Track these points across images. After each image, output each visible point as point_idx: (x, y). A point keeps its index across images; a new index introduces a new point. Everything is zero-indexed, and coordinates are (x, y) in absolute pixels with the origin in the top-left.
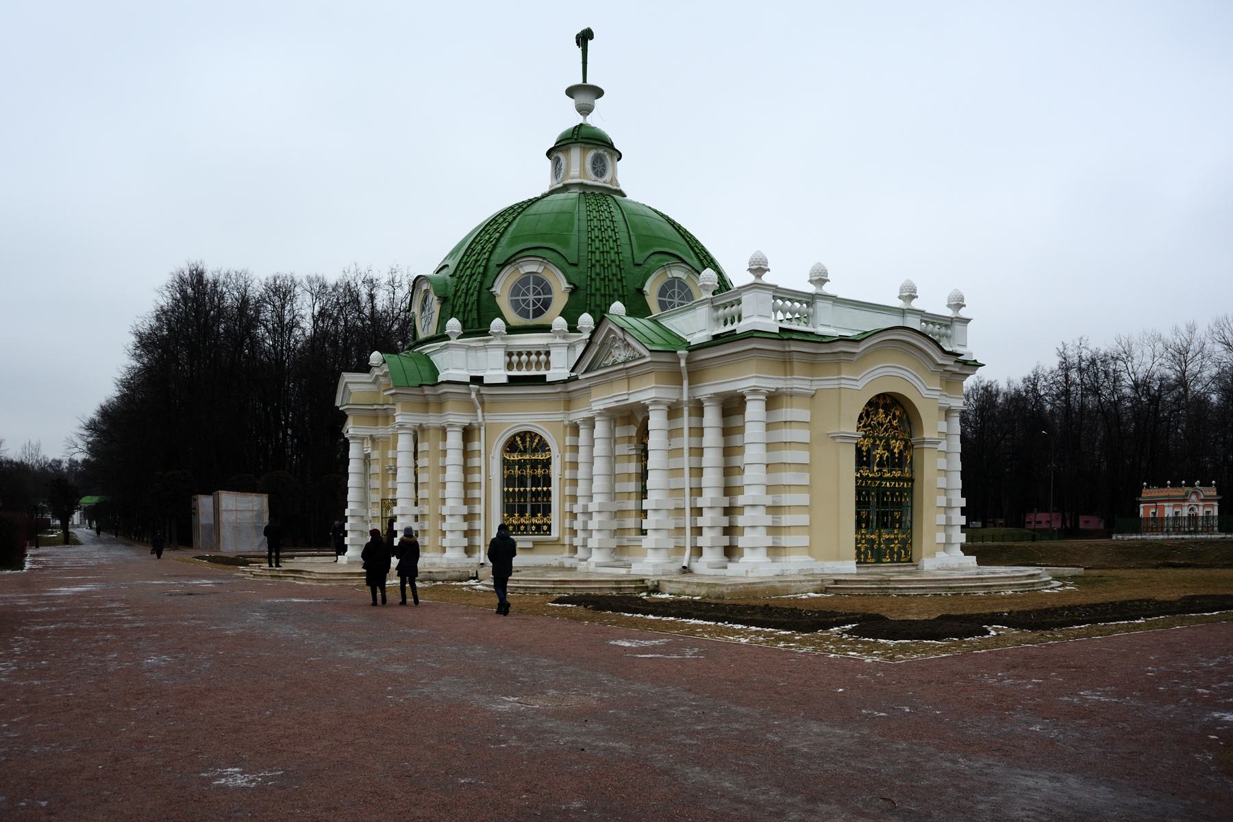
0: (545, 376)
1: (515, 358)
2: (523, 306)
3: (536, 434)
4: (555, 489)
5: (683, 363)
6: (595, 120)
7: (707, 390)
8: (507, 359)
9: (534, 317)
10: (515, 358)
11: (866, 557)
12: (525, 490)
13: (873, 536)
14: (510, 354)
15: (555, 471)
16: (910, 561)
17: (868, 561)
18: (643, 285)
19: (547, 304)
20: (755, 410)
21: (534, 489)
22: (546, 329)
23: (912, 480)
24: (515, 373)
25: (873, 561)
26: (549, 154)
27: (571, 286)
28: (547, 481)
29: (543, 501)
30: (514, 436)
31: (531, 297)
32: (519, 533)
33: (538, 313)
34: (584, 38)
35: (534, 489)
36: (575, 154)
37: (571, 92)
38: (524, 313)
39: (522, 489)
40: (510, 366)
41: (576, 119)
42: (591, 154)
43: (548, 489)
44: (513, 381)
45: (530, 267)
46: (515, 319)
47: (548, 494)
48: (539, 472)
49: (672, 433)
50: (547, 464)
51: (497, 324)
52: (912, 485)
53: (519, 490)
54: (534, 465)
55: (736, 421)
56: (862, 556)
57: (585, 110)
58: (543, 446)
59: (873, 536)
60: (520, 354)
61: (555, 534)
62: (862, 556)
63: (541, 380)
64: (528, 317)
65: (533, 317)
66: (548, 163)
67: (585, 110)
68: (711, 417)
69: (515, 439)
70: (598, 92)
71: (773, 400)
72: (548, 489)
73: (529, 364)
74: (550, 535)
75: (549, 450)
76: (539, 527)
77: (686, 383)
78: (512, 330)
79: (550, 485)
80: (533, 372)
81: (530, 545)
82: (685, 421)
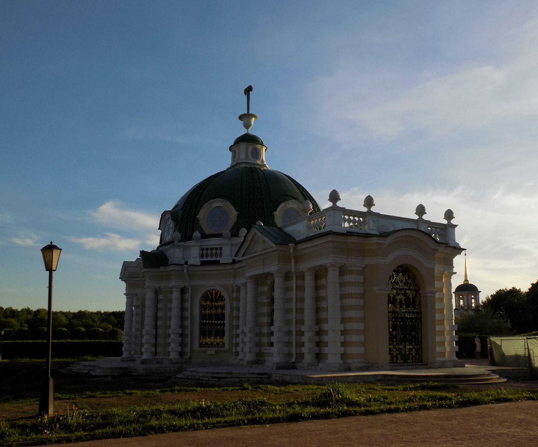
0: (219, 261)
4: (227, 322)
5: (292, 251)
6: (252, 131)
7: (304, 266)
8: (201, 252)
10: (205, 252)
11: (397, 360)
13: (401, 347)
14: (202, 250)
15: (227, 311)
16: (421, 361)
17: (399, 361)
20: (332, 276)
21: (216, 322)
23: (420, 313)
24: (205, 259)
25: (402, 362)
26: (230, 149)
28: (223, 316)
32: (208, 346)
35: (216, 322)
36: (243, 146)
37: (241, 117)
40: (202, 256)
41: (243, 131)
42: (251, 148)
43: (223, 322)
46: (207, 231)
47: (223, 325)
48: (219, 311)
49: (286, 290)
50: (223, 308)
51: (197, 234)
52: (421, 316)
53: (209, 322)
54: (216, 308)
55: (322, 282)
56: (395, 359)
57: (247, 126)
58: (222, 298)
59: (401, 347)
61: (227, 346)
62: (395, 359)
63: (219, 261)
66: (230, 154)
67: (247, 126)
68: (309, 281)
69: (207, 295)
71: (342, 271)
74: (224, 347)
77: (293, 261)
78: (204, 236)
79: (224, 320)
80: (214, 259)
81: (214, 352)
82: (293, 283)
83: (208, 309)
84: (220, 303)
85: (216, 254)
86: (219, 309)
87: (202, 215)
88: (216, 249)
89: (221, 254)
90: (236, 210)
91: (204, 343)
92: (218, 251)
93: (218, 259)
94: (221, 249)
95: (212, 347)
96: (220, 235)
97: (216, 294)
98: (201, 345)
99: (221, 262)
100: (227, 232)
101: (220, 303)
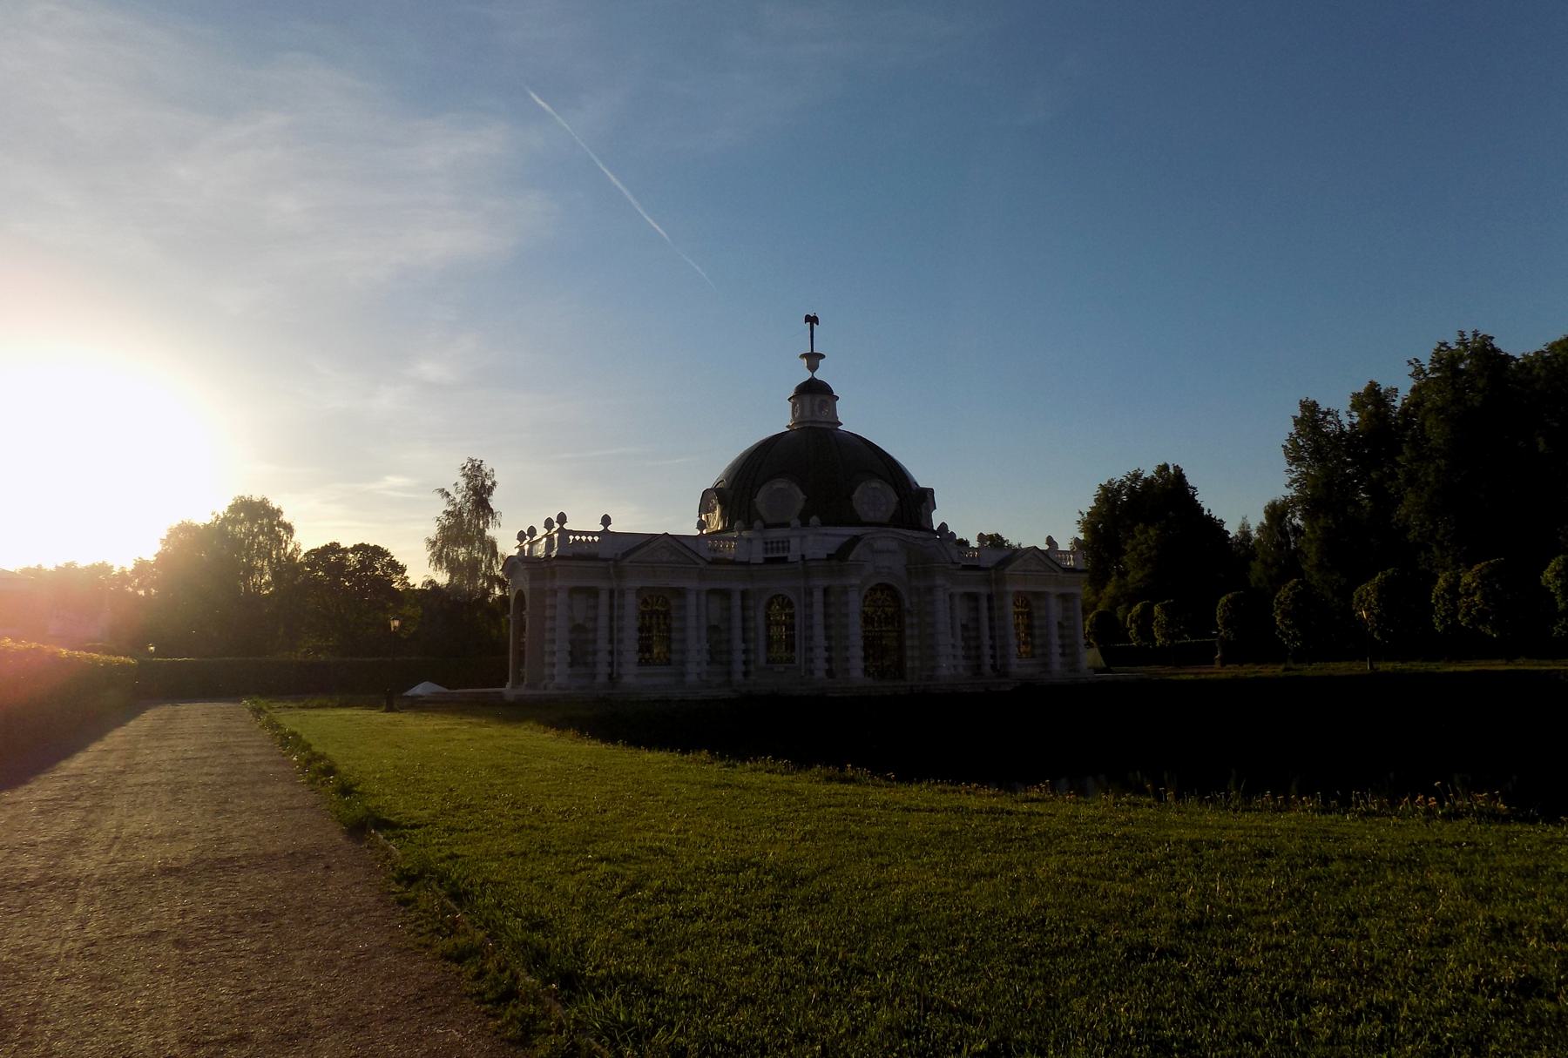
0: (787, 557)
1: (769, 546)
6: (819, 375)
10: (769, 546)
14: (766, 543)
18: (853, 491)
24: (769, 555)
27: (805, 497)
34: (812, 320)
36: (807, 399)
40: (766, 550)
41: (807, 375)
42: (818, 399)
44: (768, 561)
45: (780, 484)
51: (758, 524)
57: (813, 367)
60: (772, 542)
63: (787, 557)
67: (813, 367)
70: (822, 356)
73: (778, 549)
78: (767, 526)
80: (781, 554)
81: (783, 669)
85: (784, 548)
87: (761, 500)
88: (783, 542)
89: (789, 548)
90: (805, 494)
91: (771, 659)
92: (786, 545)
93: (785, 555)
94: (789, 542)
96: (785, 525)
97: (783, 599)
98: (768, 661)
99: (790, 559)
100: (796, 522)
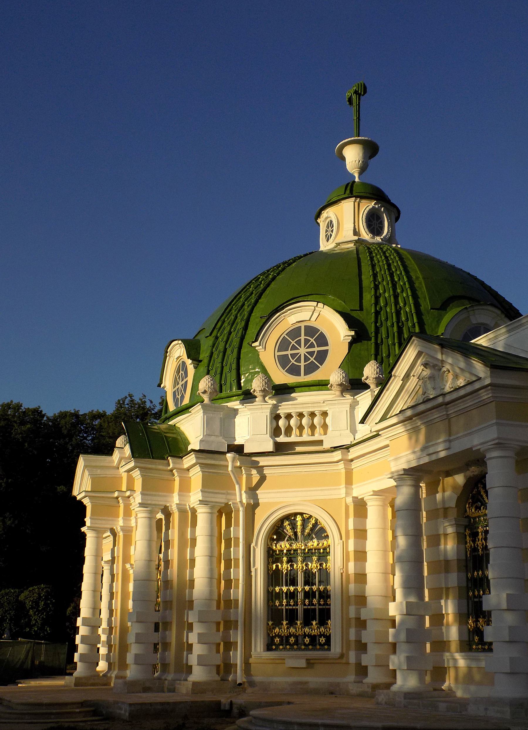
2: (293, 361)
3: (311, 517)
9: (305, 374)
12: (296, 590)
19: (322, 357)
21: (307, 588)
22: (322, 385)
24: (282, 439)
29: (320, 605)
30: (282, 520)
31: (303, 351)
32: (288, 647)
33: (311, 369)
38: (294, 371)
39: (292, 588)
43: (325, 589)
54: (308, 555)
61: (336, 648)
64: (299, 374)
65: (305, 374)
72: (325, 589)
74: (329, 649)
75: (327, 537)
76: (313, 639)
83: (285, 559)
84: (314, 543)
86: (315, 558)
95: (299, 649)
97: (305, 521)
101: (314, 543)
